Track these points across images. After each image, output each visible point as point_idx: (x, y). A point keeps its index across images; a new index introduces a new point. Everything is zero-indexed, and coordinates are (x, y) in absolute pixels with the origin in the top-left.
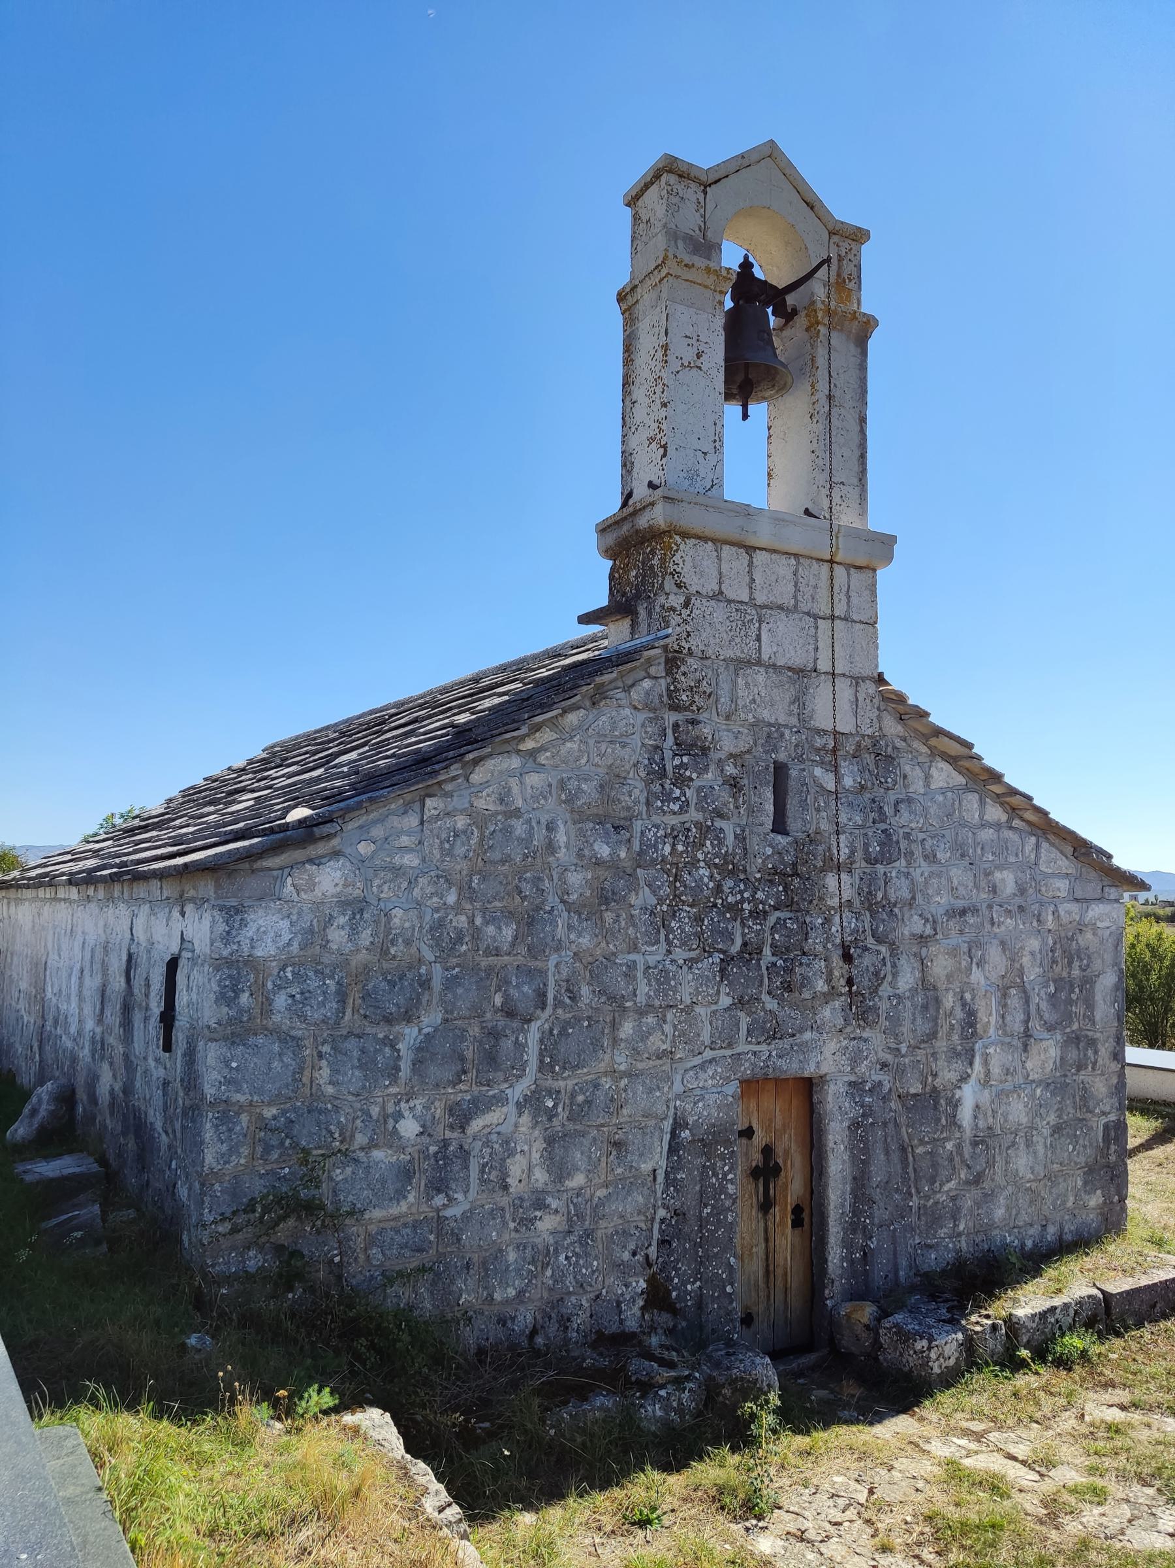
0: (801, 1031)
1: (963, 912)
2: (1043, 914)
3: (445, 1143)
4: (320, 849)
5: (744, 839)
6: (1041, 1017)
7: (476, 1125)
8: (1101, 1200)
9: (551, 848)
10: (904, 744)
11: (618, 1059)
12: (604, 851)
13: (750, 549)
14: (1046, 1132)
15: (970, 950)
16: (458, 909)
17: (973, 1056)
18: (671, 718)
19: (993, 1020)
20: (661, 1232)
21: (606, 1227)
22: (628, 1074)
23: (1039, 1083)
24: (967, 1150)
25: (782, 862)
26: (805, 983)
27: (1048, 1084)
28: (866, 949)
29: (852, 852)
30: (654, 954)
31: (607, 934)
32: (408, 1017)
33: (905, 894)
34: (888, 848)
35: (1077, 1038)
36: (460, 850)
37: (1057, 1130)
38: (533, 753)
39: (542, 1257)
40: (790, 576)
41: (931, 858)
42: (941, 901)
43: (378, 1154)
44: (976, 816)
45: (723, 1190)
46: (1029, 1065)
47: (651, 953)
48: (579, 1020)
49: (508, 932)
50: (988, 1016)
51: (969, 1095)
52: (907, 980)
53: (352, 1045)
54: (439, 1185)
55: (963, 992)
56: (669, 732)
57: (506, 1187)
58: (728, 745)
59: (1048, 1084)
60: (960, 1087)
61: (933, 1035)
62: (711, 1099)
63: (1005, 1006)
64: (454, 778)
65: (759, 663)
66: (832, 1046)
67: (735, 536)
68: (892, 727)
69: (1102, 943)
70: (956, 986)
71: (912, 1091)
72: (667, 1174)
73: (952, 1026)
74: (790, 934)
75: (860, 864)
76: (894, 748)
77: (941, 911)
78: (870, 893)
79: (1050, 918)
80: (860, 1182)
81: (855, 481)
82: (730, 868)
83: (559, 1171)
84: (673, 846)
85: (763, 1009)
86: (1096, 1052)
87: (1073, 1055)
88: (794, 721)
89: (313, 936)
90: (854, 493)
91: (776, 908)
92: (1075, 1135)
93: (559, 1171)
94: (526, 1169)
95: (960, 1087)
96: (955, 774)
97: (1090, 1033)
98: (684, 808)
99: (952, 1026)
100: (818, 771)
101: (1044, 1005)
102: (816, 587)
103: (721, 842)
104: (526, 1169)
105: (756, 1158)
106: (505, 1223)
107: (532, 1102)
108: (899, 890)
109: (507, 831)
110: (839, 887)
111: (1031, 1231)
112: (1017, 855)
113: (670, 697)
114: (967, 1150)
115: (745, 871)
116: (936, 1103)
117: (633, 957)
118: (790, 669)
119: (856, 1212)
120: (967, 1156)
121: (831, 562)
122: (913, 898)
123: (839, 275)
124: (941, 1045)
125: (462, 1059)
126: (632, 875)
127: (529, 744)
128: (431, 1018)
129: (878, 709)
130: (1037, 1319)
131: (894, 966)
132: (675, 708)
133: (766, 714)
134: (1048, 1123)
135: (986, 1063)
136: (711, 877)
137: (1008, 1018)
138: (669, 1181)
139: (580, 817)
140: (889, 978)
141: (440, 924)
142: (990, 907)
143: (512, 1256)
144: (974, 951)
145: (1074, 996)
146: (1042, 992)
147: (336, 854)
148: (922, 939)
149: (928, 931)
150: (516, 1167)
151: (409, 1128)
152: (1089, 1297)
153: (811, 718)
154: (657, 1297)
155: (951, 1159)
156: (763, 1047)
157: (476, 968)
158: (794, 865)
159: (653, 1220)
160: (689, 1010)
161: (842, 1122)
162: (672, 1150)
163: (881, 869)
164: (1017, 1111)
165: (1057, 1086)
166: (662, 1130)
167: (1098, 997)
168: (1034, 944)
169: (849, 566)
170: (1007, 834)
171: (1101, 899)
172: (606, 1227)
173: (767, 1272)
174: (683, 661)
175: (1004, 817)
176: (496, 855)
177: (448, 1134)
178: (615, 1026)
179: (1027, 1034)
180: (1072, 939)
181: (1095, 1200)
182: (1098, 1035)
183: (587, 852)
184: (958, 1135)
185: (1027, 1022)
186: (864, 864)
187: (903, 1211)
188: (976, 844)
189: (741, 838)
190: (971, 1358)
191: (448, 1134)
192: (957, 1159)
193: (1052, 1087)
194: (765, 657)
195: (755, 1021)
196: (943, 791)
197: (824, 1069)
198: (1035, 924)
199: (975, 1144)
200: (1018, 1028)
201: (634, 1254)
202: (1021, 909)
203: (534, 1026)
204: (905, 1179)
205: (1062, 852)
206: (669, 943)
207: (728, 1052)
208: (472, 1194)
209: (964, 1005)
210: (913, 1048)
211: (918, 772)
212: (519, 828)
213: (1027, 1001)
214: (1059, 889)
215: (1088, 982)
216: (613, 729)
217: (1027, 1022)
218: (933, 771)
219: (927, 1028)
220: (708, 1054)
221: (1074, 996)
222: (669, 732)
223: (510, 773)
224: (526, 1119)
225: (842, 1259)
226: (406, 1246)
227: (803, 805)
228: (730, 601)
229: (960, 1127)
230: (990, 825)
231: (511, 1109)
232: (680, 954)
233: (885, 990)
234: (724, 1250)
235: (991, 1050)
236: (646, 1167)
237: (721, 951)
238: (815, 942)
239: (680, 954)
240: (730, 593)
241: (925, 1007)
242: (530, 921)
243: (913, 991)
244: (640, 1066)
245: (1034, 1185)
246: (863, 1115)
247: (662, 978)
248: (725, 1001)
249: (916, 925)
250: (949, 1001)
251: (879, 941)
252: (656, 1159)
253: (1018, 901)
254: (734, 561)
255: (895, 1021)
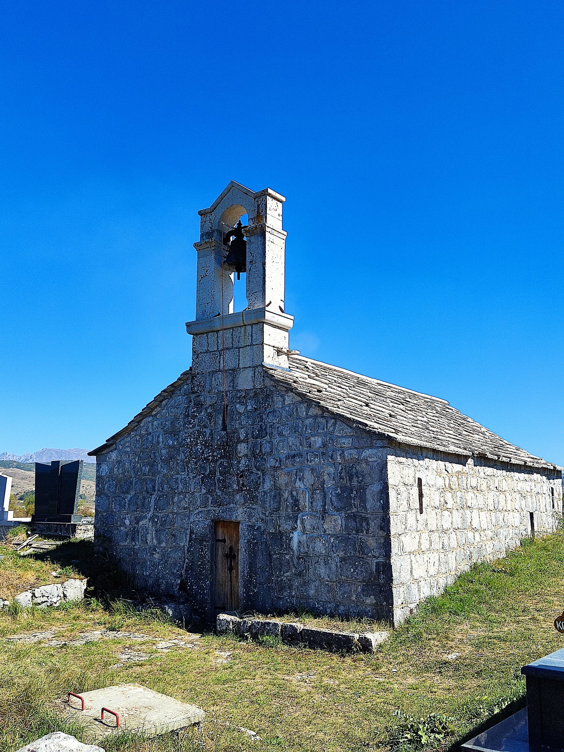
0: (229, 504)
1: (294, 456)
2: (334, 456)
3: (135, 527)
4: (112, 448)
5: (212, 434)
6: (332, 505)
7: (141, 523)
8: (374, 601)
9: (158, 443)
10: (274, 388)
11: (175, 509)
12: (171, 443)
13: (217, 331)
14: (337, 560)
15: (296, 472)
16: (138, 462)
17: (297, 519)
18: (193, 396)
19: (307, 504)
20: (186, 566)
21: (171, 561)
22: (176, 513)
23: (332, 536)
24: (295, 561)
25: (223, 441)
26: (231, 486)
27: (338, 537)
28: (252, 472)
29: (247, 435)
30: (184, 475)
31: (171, 469)
32: (128, 492)
33: (268, 450)
34: (262, 432)
35: (354, 516)
36: (137, 446)
37: (343, 559)
38: (156, 415)
39: (155, 566)
40: (230, 336)
41: (280, 434)
42: (284, 452)
43: (122, 528)
44: (304, 414)
45: (205, 557)
46: (325, 526)
47: (183, 475)
48: (163, 495)
49: (147, 469)
50: (305, 501)
51: (296, 537)
52: (267, 485)
53: (117, 498)
54: (133, 539)
55: (292, 491)
56: (193, 401)
57: (147, 543)
58: (208, 403)
59: (338, 537)
60: (293, 533)
61: (278, 509)
62: (201, 525)
63: (313, 497)
64: (137, 426)
65: (219, 371)
66: (241, 510)
67: (210, 330)
68: (268, 382)
69: (371, 469)
70: (290, 488)
71: (271, 531)
72: (188, 548)
73: (287, 506)
74: (225, 467)
75: (251, 440)
76: (270, 391)
77: (284, 456)
78: (253, 450)
79: (339, 457)
80: (252, 565)
81: (261, 289)
82: (206, 445)
83: (160, 542)
84: (190, 439)
85: (216, 495)
86: (368, 524)
87: (352, 524)
88: (231, 388)
89: (111, 470)
90: (260, 294)
91: (220, 458)
92: (355, 565)
93: (160, 542)
94: (152, 539)
95: (293, 533)
96: (296, 397)
97: (363, 514)
98: (193, 427)
99: (287, 506)
100: (238, 406)
101: (334, 499)
102: (239, 337)
103: (205, 436)
104: (152, 539)
105: (227, 551)
106: (147, 554)
107: (152, 519)
108: (266, 448)
109: (147, 439)
110: (242, 448)
111: (329, 606)
112: (324, 429)
113: (192, 390)
114: (295, 561)
115: (212, 445)
116: (281, 538)
117: (178, 476)
118: (230, 370)
119: (251, 577)
120: (295, 563)
121: (246, 325)
122: (272, 451)
123: (258, 213)
124: (283, 513)
125: (137, 505)
126: (179, 450)
127: (154, 413)
128: (133, 493)
129: (263, 377)
130: (260, 624)
131: (264, 479)
132: (193, 393)
133: (221, 389)
134: (338, 555)
135: (302, 523)
136: (201, 449)
137: (314, 504)
138: (189, 551)
139: (166, 432)
140: (262, 484)
141: (134, 467)
142: (307, 453)
143: (148, 563)
144: (299, 474)
145: (353, 495)
146: (333, 493)
147: (116, 449)
148: (275, 468)
149: (277, 464)
150: (149, 537)
151: (127, 522)
152: (291, 626)
153: (237, 386)
154: (183, 586)
155: (289, 563)
156: (217, 509)
157: (141, 479)
158: (227, 442)
159: (184, 562)
160: (193, 493)
161: (244, 540)
162: (190, 541)
163: (259, 440)
164: (320, 547)
165: (344, 539)
166: (186, 533)
167: (369, 497)
168: (332, 470)
169: (252, 325)
170: (321, 420)
171: (371, 447)
172: (171, 561)
173: (231, 593)
174: (196, 377)
175: (320, 412)
176: (145, 447)
177: (136, 525)
178: (173, 499)
179: (325, 511)
180: (352, 467)
181: (370, 600)
182: (369, 516)
183: (167, 444)
184: (292, 553)
185: (324, 506)
186: (252, 439)
187: (269, 580)
188: (303, 426)
189: (211, 434)
190: (240, 633)
191: (136, 525)
192: (291, 564)
193: (340, 538)
194: (221, 368)
195: (213, 499)
196: (289, 405)
197: (239, 519)
198: (330, 460)
199: (299, 558)
200: (320, 508)
201: (178, 571)
202: (323, 454)
203: (153, 496)
204: (271, 568)
205: (348, 425)
206: (188, 471)
207: (206, 509)
208: (140, 543)
209: (293, 496)
210: (271, 514)
211: (280, 398)
212: (150, 438)
213: (325, 497)
214: (344, 443)
215: (362, 489)
216: (175, 404)
217: (324, 506)
218: (286, 397)
219: (275, 505)
220: (200, 509)
221: (353, 495)
222: (193, 401)
223: (149, 422)
224: (150, 524)
225: (244, 593)
226: (126, 554)
227: (232, 419)
228: (210, 352)
229: (292, 550)
230: (311, 417)
231: (147, 520)
232: (191, 475)
233: (261, 489)
234: (205, 578)
235: (306, 518)
236: (182, 544)
237: (203, 474)
238: (234, 470)
239: (191, 475)
240: (210, 350)
241: (275, 496)
242: (152, 465)
243: (271, 490)
244: (180, 511)
245: (330, 584)
246: (254, 539)
247: (185, 483)
248: (204, 491)
249: (272, 462)
250: (286, 495)
251: (258, 470)
252: (184, 543)
253: (321, 450)
254: (212, 337)
255: (264, 502)
